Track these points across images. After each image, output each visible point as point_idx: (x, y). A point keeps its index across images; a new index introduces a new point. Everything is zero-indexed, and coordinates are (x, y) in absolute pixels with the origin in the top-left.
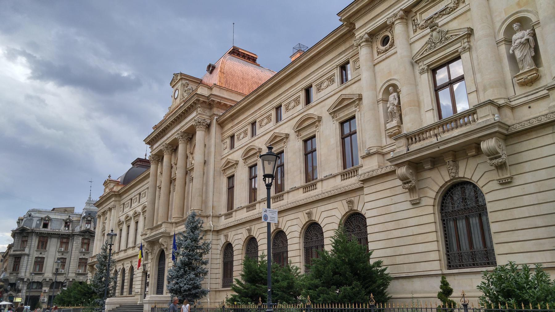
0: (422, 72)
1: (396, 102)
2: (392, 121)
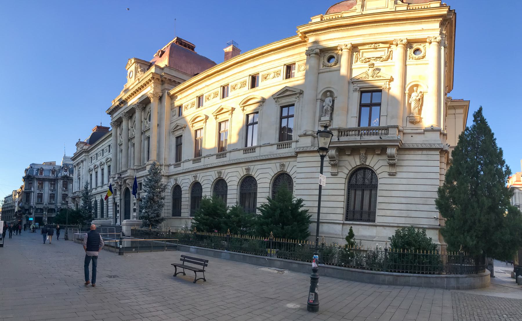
0: (355, 90)
1: (331, 104)
2: (325, 116)
